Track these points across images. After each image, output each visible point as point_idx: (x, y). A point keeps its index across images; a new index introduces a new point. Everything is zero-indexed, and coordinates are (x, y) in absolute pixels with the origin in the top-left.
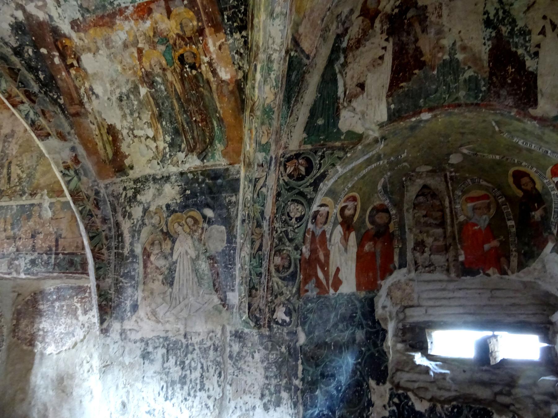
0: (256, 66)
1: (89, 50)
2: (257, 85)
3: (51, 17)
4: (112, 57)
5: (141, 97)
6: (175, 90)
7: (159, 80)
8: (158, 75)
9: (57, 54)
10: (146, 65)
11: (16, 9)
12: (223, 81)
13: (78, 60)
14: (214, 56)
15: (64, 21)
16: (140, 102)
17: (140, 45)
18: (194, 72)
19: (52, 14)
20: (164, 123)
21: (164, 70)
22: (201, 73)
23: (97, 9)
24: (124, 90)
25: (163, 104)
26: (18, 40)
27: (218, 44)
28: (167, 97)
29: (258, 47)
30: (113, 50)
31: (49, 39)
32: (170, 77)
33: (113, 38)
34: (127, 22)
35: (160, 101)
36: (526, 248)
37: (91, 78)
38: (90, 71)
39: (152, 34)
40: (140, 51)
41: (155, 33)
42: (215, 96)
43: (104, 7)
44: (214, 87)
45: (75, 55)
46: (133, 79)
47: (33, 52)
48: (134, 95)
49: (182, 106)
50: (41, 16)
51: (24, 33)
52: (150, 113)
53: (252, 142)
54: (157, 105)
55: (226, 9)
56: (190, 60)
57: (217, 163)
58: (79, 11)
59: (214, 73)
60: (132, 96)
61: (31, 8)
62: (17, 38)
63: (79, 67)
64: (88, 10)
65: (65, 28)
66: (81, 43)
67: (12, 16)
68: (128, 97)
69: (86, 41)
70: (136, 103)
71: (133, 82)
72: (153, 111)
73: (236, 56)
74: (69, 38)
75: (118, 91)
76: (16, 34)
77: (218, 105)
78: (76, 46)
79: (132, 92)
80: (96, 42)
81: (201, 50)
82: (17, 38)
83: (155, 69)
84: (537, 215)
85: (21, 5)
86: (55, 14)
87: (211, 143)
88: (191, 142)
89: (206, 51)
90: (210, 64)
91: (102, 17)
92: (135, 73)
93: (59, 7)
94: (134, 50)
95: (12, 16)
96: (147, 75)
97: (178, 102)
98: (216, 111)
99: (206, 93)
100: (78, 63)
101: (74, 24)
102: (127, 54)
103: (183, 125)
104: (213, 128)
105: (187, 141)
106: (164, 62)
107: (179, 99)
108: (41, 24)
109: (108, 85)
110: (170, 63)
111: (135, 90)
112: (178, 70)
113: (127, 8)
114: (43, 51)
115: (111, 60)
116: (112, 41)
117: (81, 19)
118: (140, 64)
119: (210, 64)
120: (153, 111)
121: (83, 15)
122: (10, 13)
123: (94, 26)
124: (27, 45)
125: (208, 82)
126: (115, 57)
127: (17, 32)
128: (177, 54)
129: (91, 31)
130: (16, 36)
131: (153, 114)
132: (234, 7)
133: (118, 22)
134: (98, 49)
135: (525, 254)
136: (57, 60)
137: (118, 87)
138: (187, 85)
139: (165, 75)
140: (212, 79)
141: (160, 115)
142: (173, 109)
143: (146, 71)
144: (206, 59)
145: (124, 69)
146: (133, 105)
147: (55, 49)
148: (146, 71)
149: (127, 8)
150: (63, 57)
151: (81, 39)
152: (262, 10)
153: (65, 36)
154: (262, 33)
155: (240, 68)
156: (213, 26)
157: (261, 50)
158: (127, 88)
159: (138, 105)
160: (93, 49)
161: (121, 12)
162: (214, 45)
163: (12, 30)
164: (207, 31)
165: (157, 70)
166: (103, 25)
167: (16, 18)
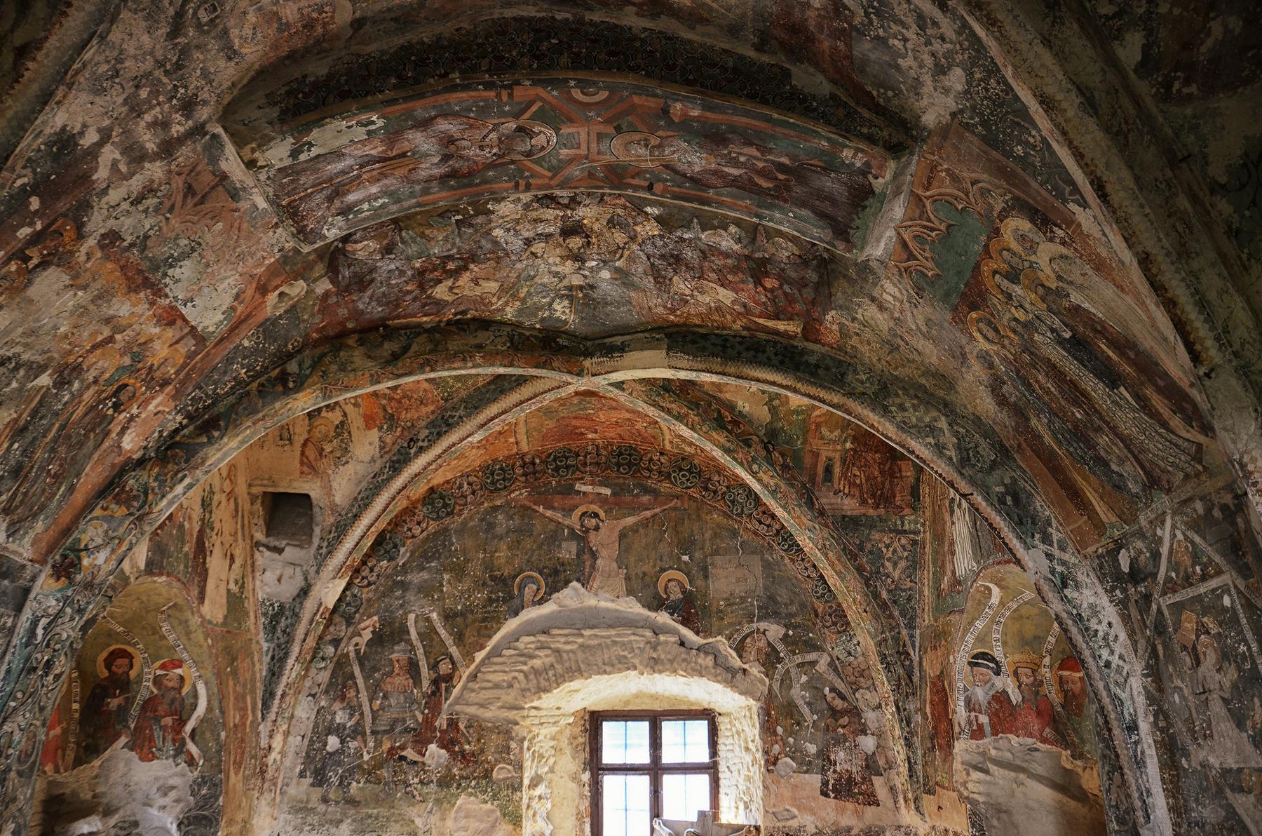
0: (185, 476)
1: (75, 277)
2: (170, 496)
3: (105, 192)
4: (81, 311)
5: (30, 385)
6: (73, 413)
7: (76, 385)
8: (82, 381)
9: (39, 226)
10: (92, 359)
11: (99, 130)
12: (119, 447)
13: (44, 264)
14: (143, 416)
15: (108, 218)
16: (20, 390)
17: (118, 337)
18: (110, 412)
19: (111, 192)
20: (16, 446)
21: (96, 382)
22: (114, 418)
23: (150, 260)
24: (25, 357)
25: (41, 418)
26: (39, 150)
27: (161, 408)
28: (56, 414)
29: (203, 462)
30: (91, 307)
31: (62, 205)
32: (88, 396)
33: (114, 300)
34: (147, 306)
35: (43, 411)
36: (90, 740)
37: (18, 299)
38: (32, 292)
39: (142, 340)
40: (110, 339)
41: (145, 343)
42: (96, 456)
43: (157, 268)
44: (106, 444)
45: (49, 254)
46: (56, 355)
47: (24, 185)
48: (27, 372)
49: (55, 440)
50: (102, 174)
51: (56, 158)
52: (15, 416)
53: (114, 557)
54: (34, 414)
55: (201, 388)
56: (123, 397)
57: (21, 550)
58: (138, 237)
59: (124, 430)
60: (22, 372)
61: (109, 154)
62: (43, 147)
63: (30, 272)
64: (144, 248)
65: (97, 223)
66: (82, 258)
67: (85, 126)
68: (16, 369)
69: (89, 265)
70: (14, 385)
71: (51, 359)
72: (20, 416)
73: (156, 434)
74: (80, 236)
75: (18, 349)
76: (49, 144)
77: (87, 469)
78: (72, 253)
79: (31, 368)
80: (94, 280)
81: (142, 398)
82: (43, 147)
83: (92, 371)
84: (114, 703)
85: (110, 137)
86: (114, 196)
87: (35, 516)
88: (19, 498)
89: (147, 402)
90: (132, 418)
91: (140, 272)
92: (70, 352)
93: (132, 203)
94: (106, 332)
95: (85, 126)
96: (74, 369)
97: (58, 430)
98: (78, 476)
99: (91, 444)
100: (36, 266)
101: (112, 237)
102: (94, 327)
103: (32, 467)
104: (55, 494)
105: (15, 494)
106: (107, 375)
107: (62, 427)
108: (85, 179)
109: (20, 330)
110: (109, 382)
111: (37, 369)
112: (104, 395)
113: (167, 296)
114: (35, 203)
115: (72, 314)
116: (109, 301)
117: (125, 244)
118: (88, 351)
119: (132, 418)
120: (20, 416)
121: (132, 245)
122: (90, 121)
123: (122, 268)
124: (34, 172)
125: (107, 434)
126: (81, 315)
127: (55, 143)
128: (126, 381)
129: (110, 266)
130: (45, 144)
131: (16, 421)
132: (207, 394)
133: (142, 295)
134: (84, 288)
135: (87, 748)
136: (24, 232)
137: (26, 345)
138: (88, 418)
139: (88, 387)
140: (114, 435)
141: (24, 429)
142: (44, 436)
143: (80, 364)
144: (135, 411)
145: (66, 336)
146: (9, 384)
147: (47, 222)
148: (80, 364)
149: (167, 296)
150: (35, 239)
151: (89, 256)
152: (239, 438)
153: (80, 227)
154: (219, 455)
155: (145, 448)
156: (177, 390)
157: (204, 468)
158: (32, 359)
159: (13, 391)
160: (80, 281)
161: (159, 292)
162: (158, 406)
163: (55, 133)
164: (169, 389)
165: (90, 377)
166: (128, 279)
167: (82, 133)
